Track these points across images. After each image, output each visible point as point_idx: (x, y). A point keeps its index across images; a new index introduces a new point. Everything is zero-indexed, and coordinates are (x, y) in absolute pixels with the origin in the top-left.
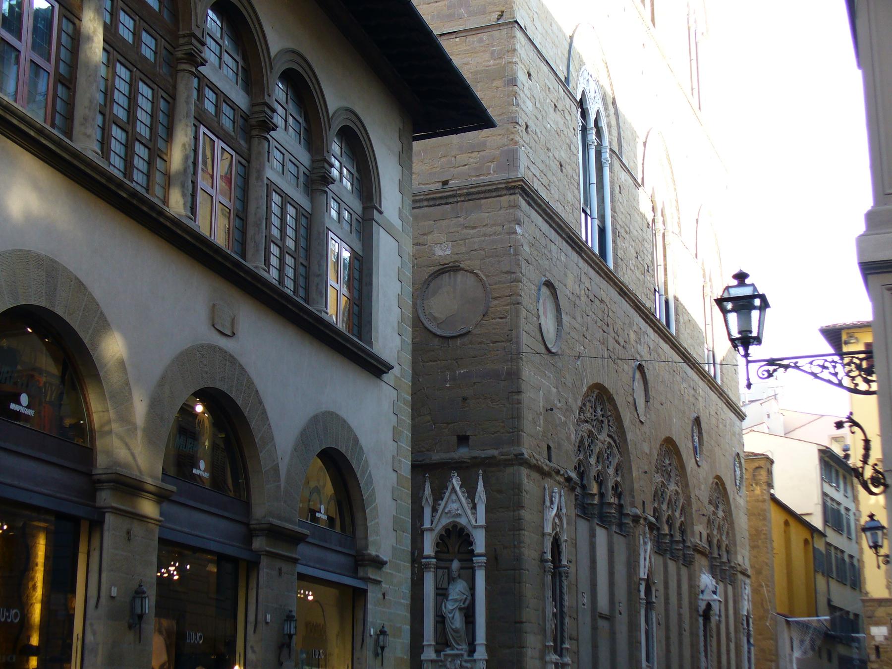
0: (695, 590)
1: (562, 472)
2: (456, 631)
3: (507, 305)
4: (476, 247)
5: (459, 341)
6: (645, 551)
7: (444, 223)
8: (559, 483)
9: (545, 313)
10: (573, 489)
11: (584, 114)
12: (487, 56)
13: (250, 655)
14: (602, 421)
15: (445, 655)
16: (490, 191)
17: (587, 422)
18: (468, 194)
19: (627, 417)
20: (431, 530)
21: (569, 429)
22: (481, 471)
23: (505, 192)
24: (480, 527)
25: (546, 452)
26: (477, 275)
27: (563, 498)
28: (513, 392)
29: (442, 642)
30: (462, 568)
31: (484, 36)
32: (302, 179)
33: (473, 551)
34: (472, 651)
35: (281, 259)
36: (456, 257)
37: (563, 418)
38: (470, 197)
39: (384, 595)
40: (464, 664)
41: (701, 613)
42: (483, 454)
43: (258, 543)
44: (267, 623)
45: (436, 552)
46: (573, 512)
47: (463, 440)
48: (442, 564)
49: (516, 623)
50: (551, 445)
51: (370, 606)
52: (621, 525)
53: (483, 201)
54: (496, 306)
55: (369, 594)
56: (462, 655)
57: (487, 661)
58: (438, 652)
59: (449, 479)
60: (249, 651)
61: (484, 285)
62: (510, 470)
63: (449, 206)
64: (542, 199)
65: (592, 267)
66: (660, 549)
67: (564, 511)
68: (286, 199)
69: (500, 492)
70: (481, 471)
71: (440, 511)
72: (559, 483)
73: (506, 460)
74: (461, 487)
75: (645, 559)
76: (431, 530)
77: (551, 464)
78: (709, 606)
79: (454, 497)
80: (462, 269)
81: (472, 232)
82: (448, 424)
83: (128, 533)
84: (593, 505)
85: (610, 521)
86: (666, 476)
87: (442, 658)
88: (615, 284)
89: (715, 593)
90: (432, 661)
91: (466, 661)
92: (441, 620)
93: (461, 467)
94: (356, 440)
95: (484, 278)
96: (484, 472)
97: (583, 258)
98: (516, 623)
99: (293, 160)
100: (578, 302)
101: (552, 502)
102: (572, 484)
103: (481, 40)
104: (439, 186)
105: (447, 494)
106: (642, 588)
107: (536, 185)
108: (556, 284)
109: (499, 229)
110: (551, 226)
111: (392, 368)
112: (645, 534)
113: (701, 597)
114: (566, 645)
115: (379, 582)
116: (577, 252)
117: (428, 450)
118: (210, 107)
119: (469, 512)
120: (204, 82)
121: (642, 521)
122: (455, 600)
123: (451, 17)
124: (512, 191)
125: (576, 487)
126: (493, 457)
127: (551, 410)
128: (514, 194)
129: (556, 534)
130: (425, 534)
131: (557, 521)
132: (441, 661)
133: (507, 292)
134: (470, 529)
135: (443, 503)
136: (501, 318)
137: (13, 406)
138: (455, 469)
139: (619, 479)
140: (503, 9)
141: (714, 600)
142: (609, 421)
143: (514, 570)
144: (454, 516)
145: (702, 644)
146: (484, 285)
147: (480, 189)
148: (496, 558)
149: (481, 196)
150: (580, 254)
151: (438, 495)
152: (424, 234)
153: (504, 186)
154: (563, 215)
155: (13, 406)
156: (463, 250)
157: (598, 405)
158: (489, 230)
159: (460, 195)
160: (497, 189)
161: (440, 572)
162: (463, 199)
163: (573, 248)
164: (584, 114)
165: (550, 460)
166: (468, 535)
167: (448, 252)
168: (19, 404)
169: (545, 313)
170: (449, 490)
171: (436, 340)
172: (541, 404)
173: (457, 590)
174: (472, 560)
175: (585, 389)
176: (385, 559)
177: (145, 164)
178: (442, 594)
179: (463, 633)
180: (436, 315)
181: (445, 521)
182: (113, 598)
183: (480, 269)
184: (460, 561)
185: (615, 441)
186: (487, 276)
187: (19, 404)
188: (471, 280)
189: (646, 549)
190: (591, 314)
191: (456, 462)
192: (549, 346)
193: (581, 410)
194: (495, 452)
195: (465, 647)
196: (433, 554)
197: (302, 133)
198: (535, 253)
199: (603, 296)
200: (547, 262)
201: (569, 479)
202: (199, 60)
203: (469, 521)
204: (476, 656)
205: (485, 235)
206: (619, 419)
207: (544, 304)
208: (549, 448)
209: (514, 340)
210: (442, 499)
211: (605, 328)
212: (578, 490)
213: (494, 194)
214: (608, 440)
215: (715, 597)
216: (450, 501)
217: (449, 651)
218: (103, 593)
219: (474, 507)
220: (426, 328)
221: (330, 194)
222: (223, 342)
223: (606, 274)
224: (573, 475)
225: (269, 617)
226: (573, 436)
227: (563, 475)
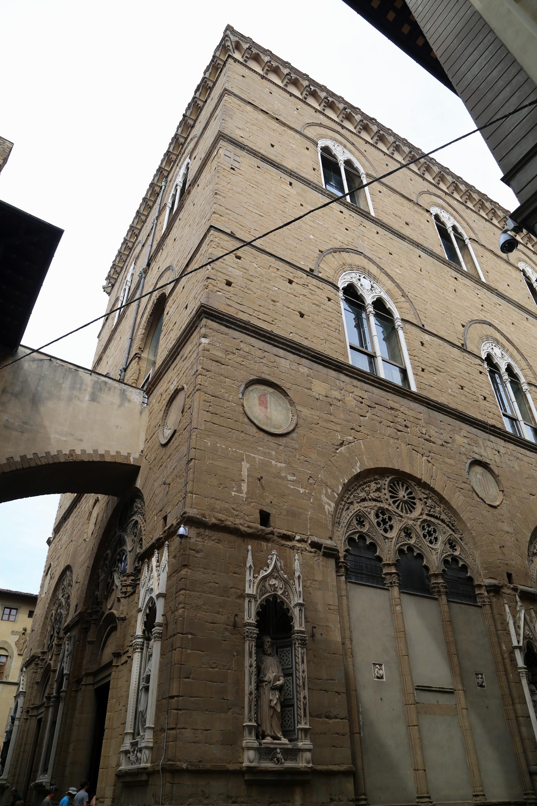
14: (415, 504)
37: (302, 490)
84: (391, 574)
85: (439, 591)
102: (322, 550)
128: (202, 319)
139: (457, 553)
227: (301, 541)
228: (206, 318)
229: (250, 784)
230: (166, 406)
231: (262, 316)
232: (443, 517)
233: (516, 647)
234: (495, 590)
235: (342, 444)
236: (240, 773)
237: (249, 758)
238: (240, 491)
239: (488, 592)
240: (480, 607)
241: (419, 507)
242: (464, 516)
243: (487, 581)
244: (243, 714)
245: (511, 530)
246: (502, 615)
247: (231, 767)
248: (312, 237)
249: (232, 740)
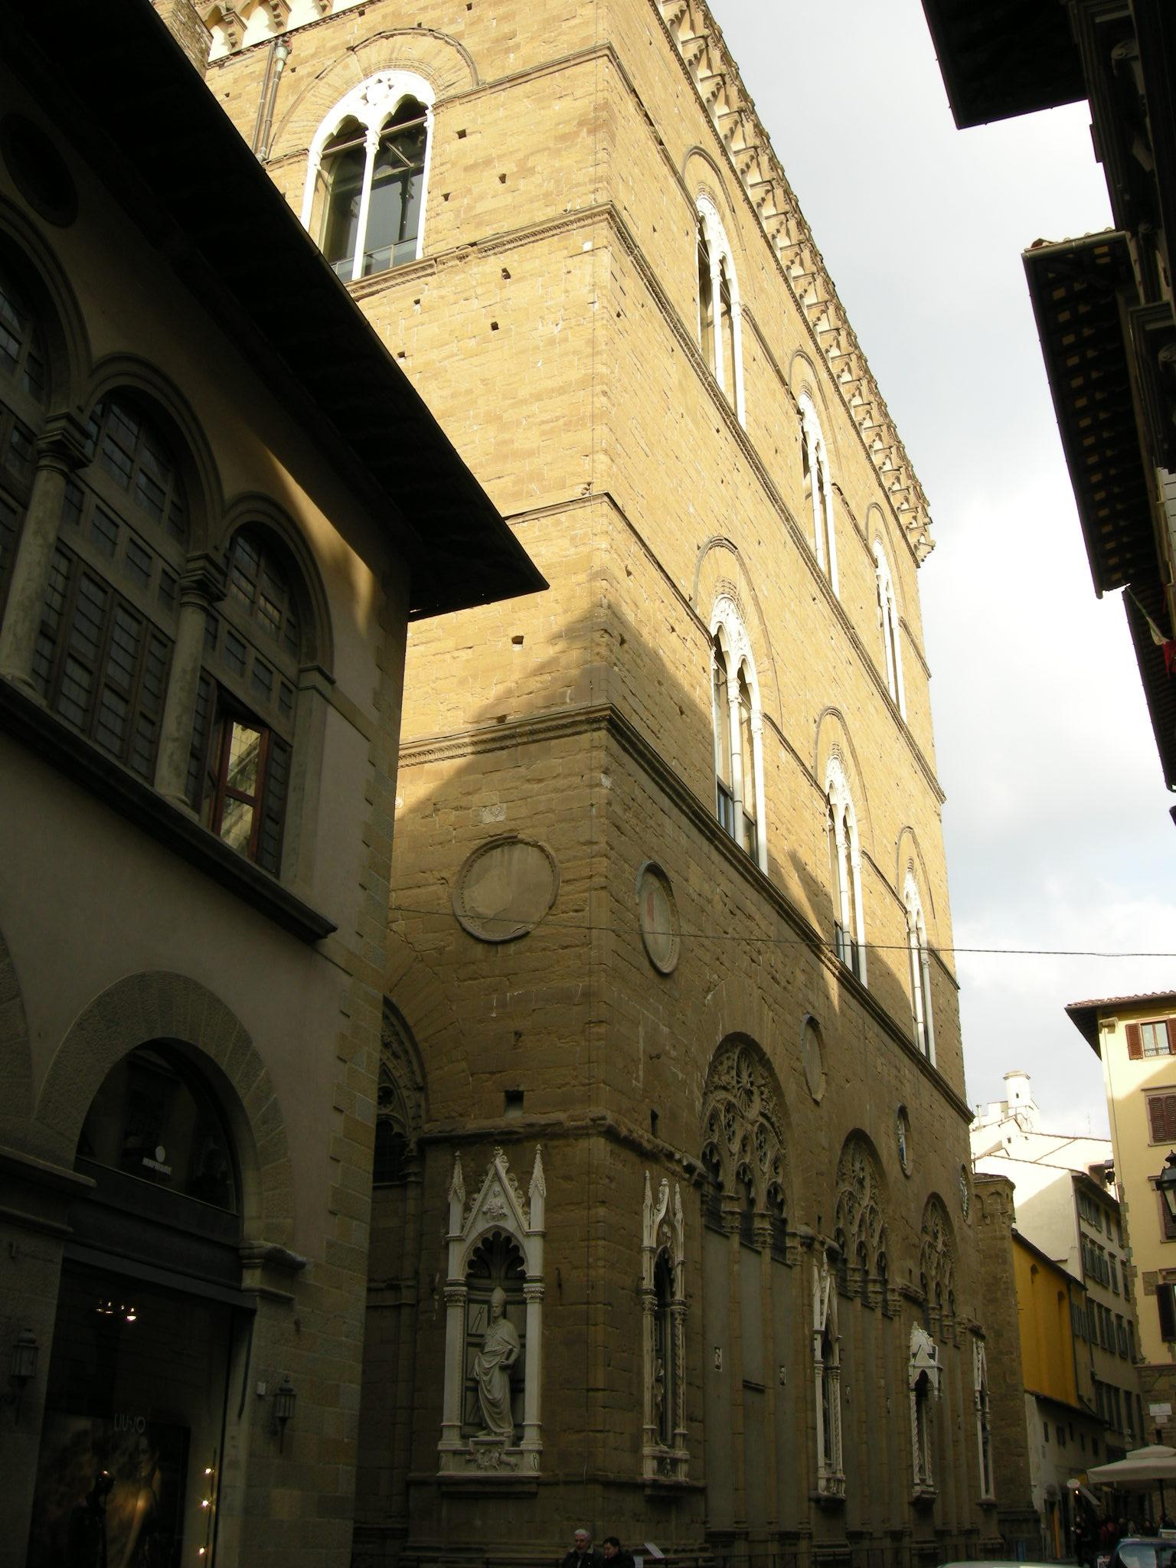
0: (906, 1354)
1: (677, 1156)
2: (494, 1404)
3: (585, 891)
4: (542, 808)
5: (512, 948)
6: (823, 1290)
7: (497, 776)
8: (673, 1173)
9: (651, 911)
10: (698, 1185)
11: (720, 657)
12: (566, 543)
14: (752, 1092)
15: (476, 1443)
16: (564, 726)
17: (725, 1088)
18: (532, 733)
19: (791, 1090)
20: (460, 1239)
21: (691, 1092)
22: (539, 1147)
23: (586, 727)
24: (535, 1234)
25: (649, 1121)
26: (542, 849)
27: (678, 1196)
28: (590, 1022)
29: (474, 1422)
30: (506, 1303)
31: (563, 517)
33: (523, 1272)
34: (518, 1439)
36: (512, 825)
37: (680, 1076)
38: (536, 737)
39: (297, 1323)
40: (504, 1458)
41: (913, 1386)
42: (543, 1120)
45: (469, 1276)
46: (699, 1221)
47: (514, 1098)
48: (478, 1295)
49: (588, 1390)
50: (660, 1112)
51: (255, 1341)
52: (779, 1250)
53: (553, 742)
54: (568, 894)
55: (257, 1319)
56: (501, 1443)
57: (540, 1453)
58: (464, 1437)
59: (489, 1158)
61: (552, 864)
62: (583, 1144)
63: (504, 752)
64: (646, 746)
65: (731, 864)
66: (843, 1292)
67: (680, 1216)
69: (568, 1178)
70: (539, 1147)
71: (474, 1211)
72: (673, 1173)
73: (577, 1128)
74: (507, 1172)
75: (822, 1302)
76: (460, 1239)
77: (658, 1141)
78: (924, 1375)
79: (497, 1188)
80: (521, 842)
81: (536, 787)
82: (492, 1073)
84: (733, 1213)
85: (764, 1242)
86: (857, 1186)
87: (471, 1447)
88: (771, 896)
89: (932, 1356)
90: (455, 1453)
91: (509, 1453)
92: (472, 1386)
93: (509, 1139)
94: (245, 1041)
95: (552, 852)
96: (545, 1146)
97: (717, 848)
98: (588, 1390)
100: (708, 908)
101: (656, 1200)
102: (695, 1177)
103: (558, 523)
104: (494, 722)
105: (487, 1183)
106: (818, 1344)
107: (635, 722)
108: (671, 875)
109: (577, 780)
110: (663, 790)
111: (334, 929)
112: (822, 1265)
113: (912, 1362)
114: (680, 1430)
115: (288, 1302)
116: (708, 839)
117: (461, 1115)
119: (520, 1211)
121: (817, 1245)
122: (494, 1353)
123: (517, 496)
124: (595, 726)
125: (704, 1181)
126: (560, 1124)
127: (658, 1057)
128: (599, 729)
129: (665, 1250)
130: (451, 1246)
131: (666, 1229)
132: (470, 1453)
133: (586, 872)
134: (520, 1237)
135: (479, 1197)
136: (577, 911)
138: (501, 1143)
139: (780, 1180)
140: (589, 480)
141: (932, 1367)
142: (762, 1093)
143: (588, 1303)
144: (494, 1218)
145: (915, 1431)
146: (552, 864)
147: (549, 724)
148: (560, 1286)
149: (552, 734)
150: (712, 842)
151: (473, 1184)
152: (469, 794)
153: (583, 718)
154: (685, 779)
156: (524, 812)
157: (744, 1066)
158: (562, 783)
159: (522, 735)
160: (574, 724)
161: (475, 1308)
162: (525, 739)
163: (700, 831)
164: (720, 657)
165: (654, 1132)
166: (516, 1248)
167: (501, 818)
169: (651, 911)
170: (490, 1177)
171: (480, 948)
172: (641, 1048)
173: (497, 1337)
174: (521, 1290)
175: (720, 1038)
176: (300, 1258)
177: (65, 691)
178: (474, 1342)
179: (506, 1405)
180: (481, 910)
181: (482, 1226)
183: (548, 840)
184: (506, 1290)
185: (772, 1124)
186: (557, 850)
188: (533, 854)
189: (823, 1286)
190: (730, 930)
191: (502, 1133)
192: (659, 964)
193: (713, 1068)
194: (561, 1116)
195: (508, 1430)
196: (462, 1278)
198: (634, 821)
199: (751, 908)
200: (655, 839)
201: (690, 1169)
203: (520, 1226)
204: (524, 1445)
205: (556, 790)
206: (777, 1090)
207: (650, 899)
208: (654, 1117)
209: (595, 943)
210: (479, 1191)
211: (755, 955)
212: (709, 1190)
213: (569, 731)
214: (761, 1119)
215: (932, 1363)
216: (491, 1194)
217: (482, 1437)
219: (527, 1203)
220: (464, 930)
223: (756, 880)
224: (699, 1164)
226: (698, 1105)
227: (680, 1161)
228: (608, 730)
229: (650, 1500)
230: (474, 853)
231: (645, 715)
232: (774, 1119)
233: (817, 1332)
234: (809, 1243)
235: (709, 990)
236: (642, 1486)
237: (649, 1471)
238: (637, 1079)
239: (802, 1245)
240: (790, 1267)
241: (756, 1098)
242: (795, 1118)
243: (803, 1230)
244: (641, 1413)
245: (826, 1146)
246: (810, 1282)
247: (639, 1480)
248: (692, 510)
249: (636, 1448)
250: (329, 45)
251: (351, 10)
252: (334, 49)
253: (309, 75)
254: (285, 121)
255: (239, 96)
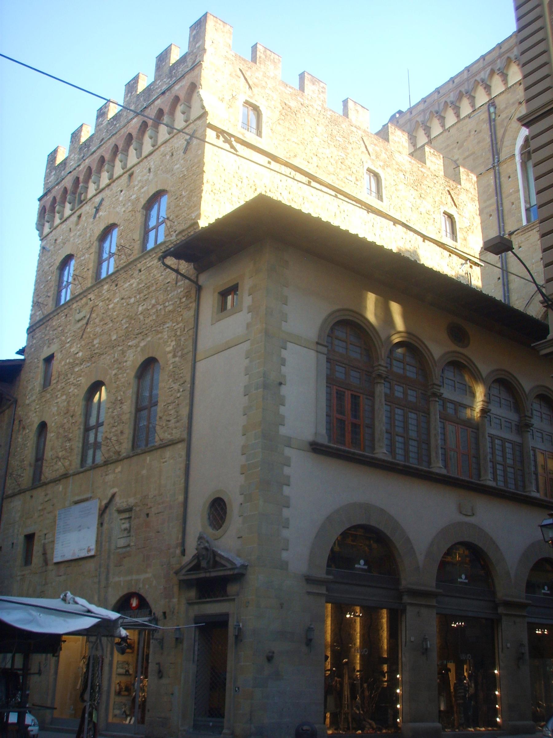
13: (501, 664)
32: (514, 428)
35: (505, 471)
43: (501, 610)
44: (508, 648)
60: (500, 661)
68: (503, 440)
83: (418, 613)
99: (507, 420)
118: (450, 411)
120: (445, 401)
137: (356, 566)
155: (356, 566)
168: (360, 564)
182: (412, 642)
187: (360, 564)
197: (512, 405)
202: (438, 394)
218: (407, 640)
221: (535, 430)
222: (467, 519)
225: (509, 645)
250: (511, 102)
251: (515, 84)
252: (513, 104)
253: (506, 117)
254: (502, 141)
255: (480, 131)
